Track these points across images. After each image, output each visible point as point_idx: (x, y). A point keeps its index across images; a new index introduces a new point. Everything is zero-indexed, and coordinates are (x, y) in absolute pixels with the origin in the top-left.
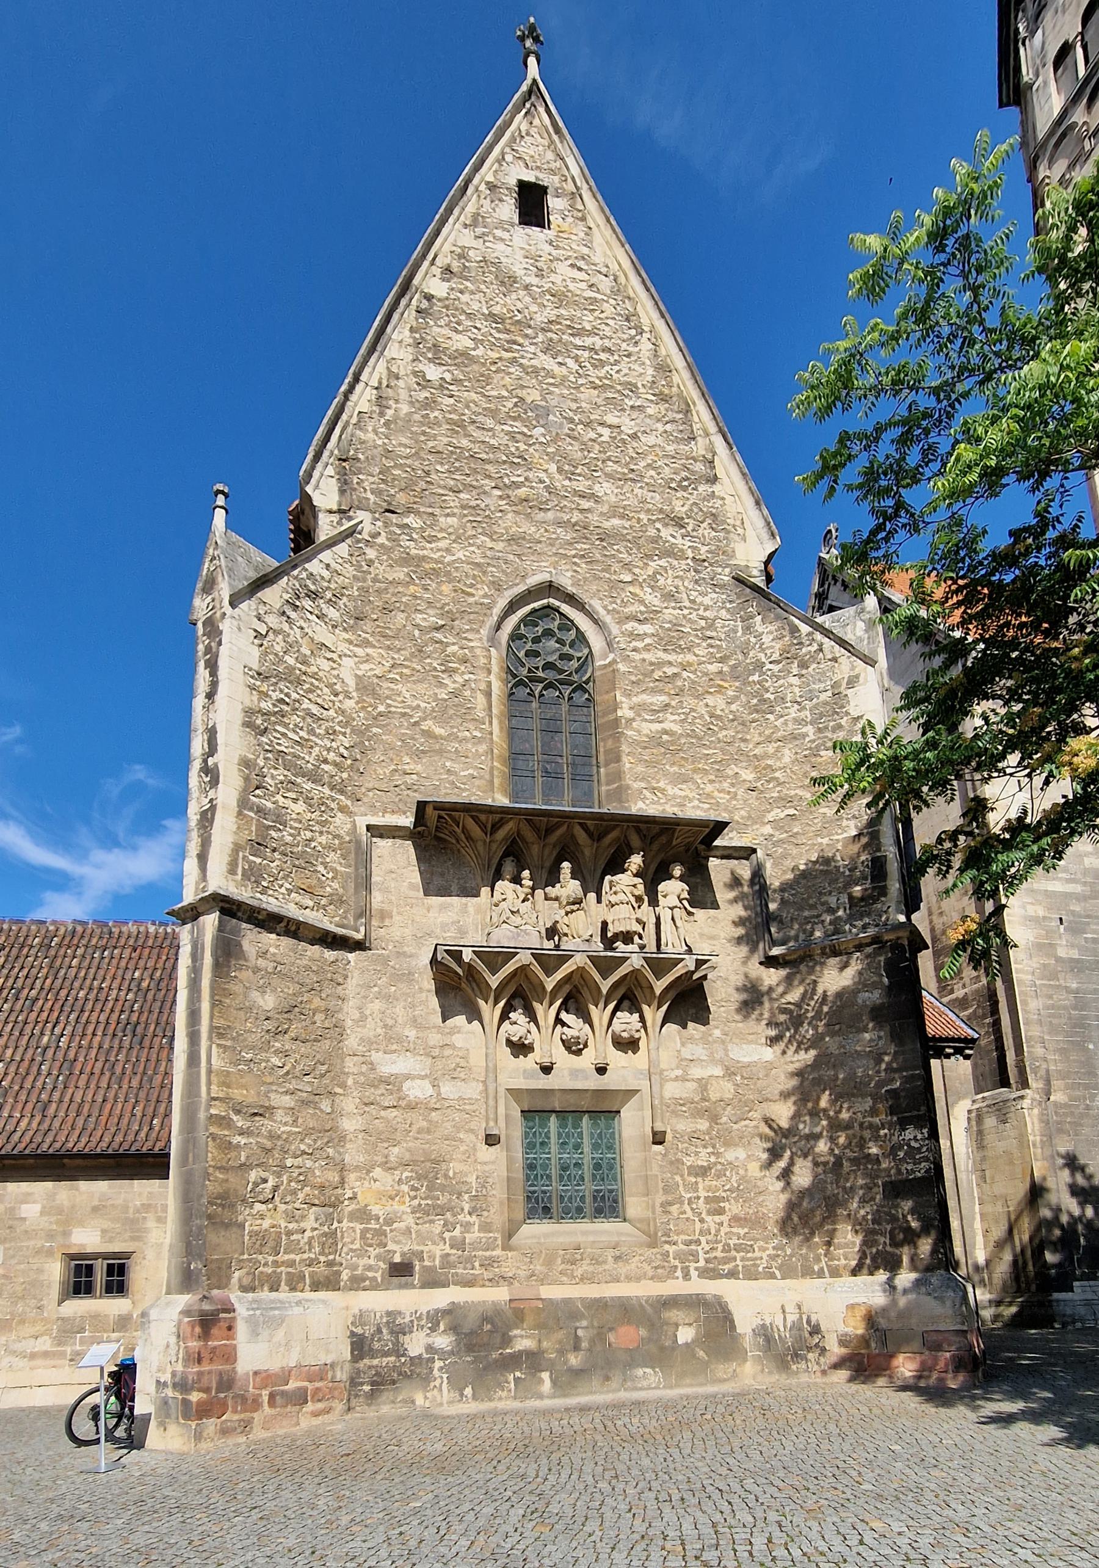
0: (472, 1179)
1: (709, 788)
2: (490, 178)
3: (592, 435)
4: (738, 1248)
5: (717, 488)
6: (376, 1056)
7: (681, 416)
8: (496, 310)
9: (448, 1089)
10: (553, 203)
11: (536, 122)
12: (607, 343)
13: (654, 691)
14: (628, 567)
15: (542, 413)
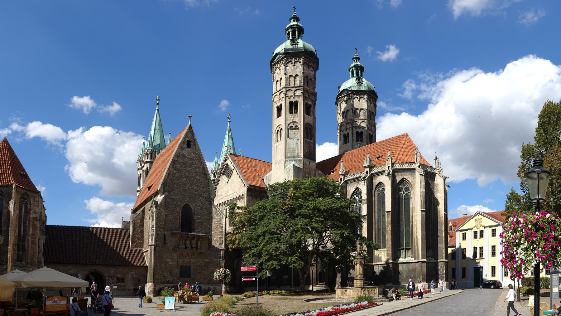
0: (176, 273)
1: (204, 228)
2: (183, 141)
3: (194, 180)
4: (203, 281)
5: (209, 187)
6: (166, 259)
7: (205, 177)
8: (183, 161)
9: (173, 263)
10: (192, 143)
11: (190, 130)
12: (197, 166)
13: (199, 216)
14: (197, 199)
15: (188, 176)
